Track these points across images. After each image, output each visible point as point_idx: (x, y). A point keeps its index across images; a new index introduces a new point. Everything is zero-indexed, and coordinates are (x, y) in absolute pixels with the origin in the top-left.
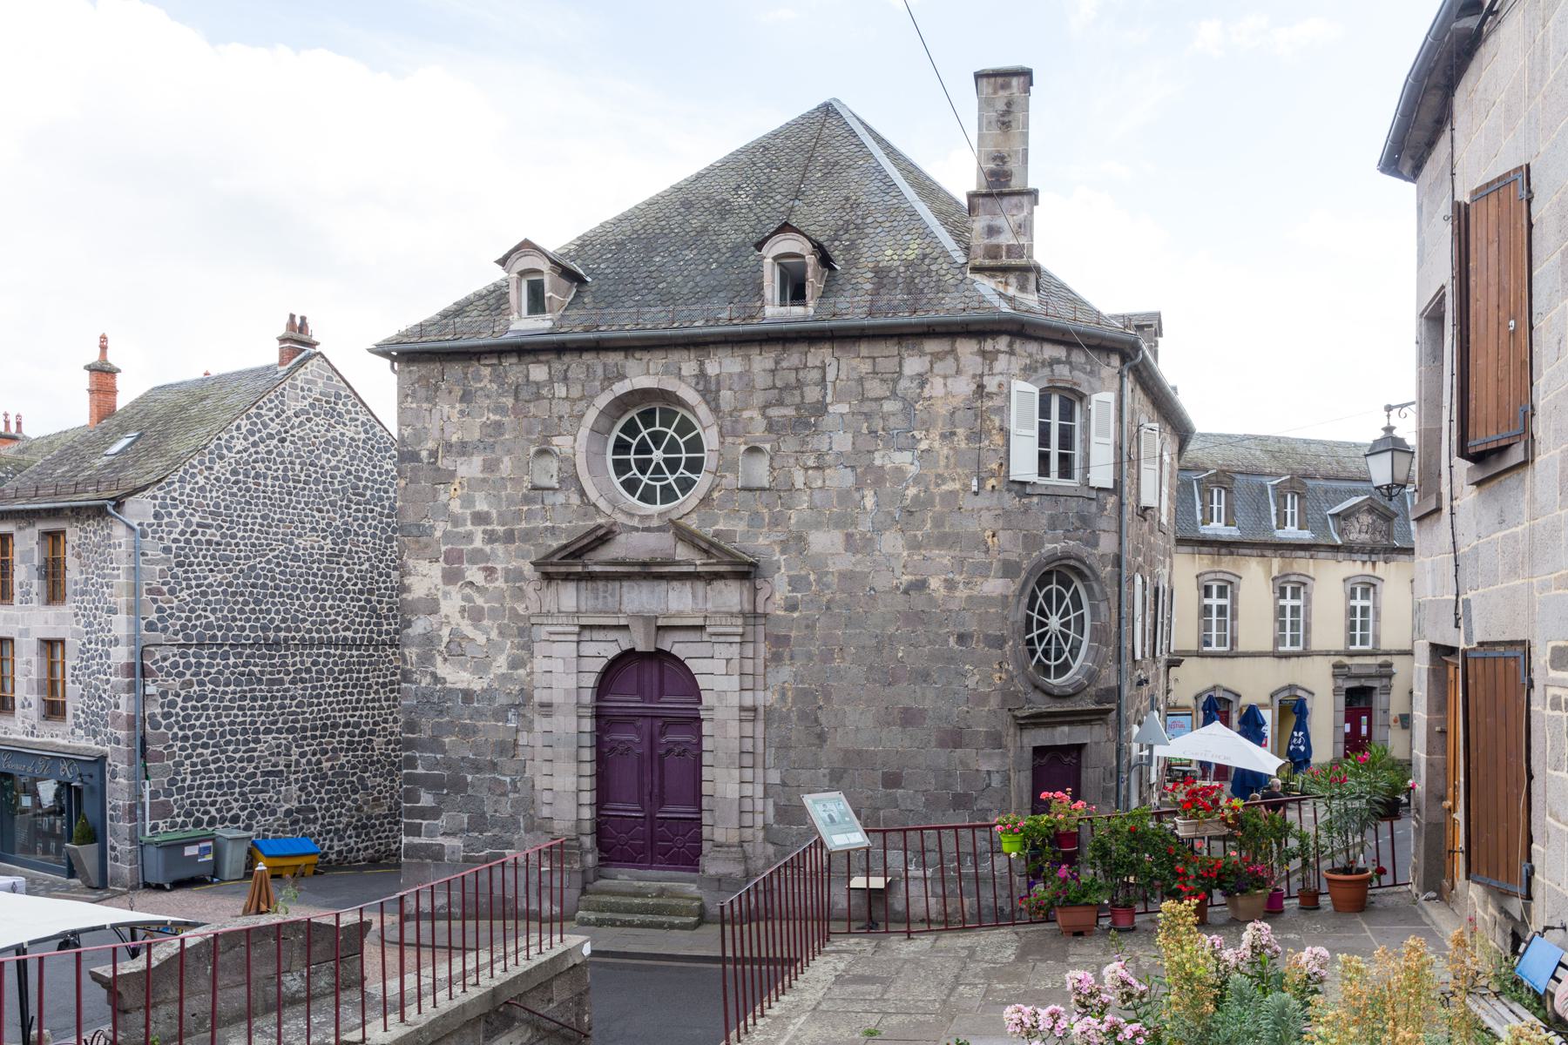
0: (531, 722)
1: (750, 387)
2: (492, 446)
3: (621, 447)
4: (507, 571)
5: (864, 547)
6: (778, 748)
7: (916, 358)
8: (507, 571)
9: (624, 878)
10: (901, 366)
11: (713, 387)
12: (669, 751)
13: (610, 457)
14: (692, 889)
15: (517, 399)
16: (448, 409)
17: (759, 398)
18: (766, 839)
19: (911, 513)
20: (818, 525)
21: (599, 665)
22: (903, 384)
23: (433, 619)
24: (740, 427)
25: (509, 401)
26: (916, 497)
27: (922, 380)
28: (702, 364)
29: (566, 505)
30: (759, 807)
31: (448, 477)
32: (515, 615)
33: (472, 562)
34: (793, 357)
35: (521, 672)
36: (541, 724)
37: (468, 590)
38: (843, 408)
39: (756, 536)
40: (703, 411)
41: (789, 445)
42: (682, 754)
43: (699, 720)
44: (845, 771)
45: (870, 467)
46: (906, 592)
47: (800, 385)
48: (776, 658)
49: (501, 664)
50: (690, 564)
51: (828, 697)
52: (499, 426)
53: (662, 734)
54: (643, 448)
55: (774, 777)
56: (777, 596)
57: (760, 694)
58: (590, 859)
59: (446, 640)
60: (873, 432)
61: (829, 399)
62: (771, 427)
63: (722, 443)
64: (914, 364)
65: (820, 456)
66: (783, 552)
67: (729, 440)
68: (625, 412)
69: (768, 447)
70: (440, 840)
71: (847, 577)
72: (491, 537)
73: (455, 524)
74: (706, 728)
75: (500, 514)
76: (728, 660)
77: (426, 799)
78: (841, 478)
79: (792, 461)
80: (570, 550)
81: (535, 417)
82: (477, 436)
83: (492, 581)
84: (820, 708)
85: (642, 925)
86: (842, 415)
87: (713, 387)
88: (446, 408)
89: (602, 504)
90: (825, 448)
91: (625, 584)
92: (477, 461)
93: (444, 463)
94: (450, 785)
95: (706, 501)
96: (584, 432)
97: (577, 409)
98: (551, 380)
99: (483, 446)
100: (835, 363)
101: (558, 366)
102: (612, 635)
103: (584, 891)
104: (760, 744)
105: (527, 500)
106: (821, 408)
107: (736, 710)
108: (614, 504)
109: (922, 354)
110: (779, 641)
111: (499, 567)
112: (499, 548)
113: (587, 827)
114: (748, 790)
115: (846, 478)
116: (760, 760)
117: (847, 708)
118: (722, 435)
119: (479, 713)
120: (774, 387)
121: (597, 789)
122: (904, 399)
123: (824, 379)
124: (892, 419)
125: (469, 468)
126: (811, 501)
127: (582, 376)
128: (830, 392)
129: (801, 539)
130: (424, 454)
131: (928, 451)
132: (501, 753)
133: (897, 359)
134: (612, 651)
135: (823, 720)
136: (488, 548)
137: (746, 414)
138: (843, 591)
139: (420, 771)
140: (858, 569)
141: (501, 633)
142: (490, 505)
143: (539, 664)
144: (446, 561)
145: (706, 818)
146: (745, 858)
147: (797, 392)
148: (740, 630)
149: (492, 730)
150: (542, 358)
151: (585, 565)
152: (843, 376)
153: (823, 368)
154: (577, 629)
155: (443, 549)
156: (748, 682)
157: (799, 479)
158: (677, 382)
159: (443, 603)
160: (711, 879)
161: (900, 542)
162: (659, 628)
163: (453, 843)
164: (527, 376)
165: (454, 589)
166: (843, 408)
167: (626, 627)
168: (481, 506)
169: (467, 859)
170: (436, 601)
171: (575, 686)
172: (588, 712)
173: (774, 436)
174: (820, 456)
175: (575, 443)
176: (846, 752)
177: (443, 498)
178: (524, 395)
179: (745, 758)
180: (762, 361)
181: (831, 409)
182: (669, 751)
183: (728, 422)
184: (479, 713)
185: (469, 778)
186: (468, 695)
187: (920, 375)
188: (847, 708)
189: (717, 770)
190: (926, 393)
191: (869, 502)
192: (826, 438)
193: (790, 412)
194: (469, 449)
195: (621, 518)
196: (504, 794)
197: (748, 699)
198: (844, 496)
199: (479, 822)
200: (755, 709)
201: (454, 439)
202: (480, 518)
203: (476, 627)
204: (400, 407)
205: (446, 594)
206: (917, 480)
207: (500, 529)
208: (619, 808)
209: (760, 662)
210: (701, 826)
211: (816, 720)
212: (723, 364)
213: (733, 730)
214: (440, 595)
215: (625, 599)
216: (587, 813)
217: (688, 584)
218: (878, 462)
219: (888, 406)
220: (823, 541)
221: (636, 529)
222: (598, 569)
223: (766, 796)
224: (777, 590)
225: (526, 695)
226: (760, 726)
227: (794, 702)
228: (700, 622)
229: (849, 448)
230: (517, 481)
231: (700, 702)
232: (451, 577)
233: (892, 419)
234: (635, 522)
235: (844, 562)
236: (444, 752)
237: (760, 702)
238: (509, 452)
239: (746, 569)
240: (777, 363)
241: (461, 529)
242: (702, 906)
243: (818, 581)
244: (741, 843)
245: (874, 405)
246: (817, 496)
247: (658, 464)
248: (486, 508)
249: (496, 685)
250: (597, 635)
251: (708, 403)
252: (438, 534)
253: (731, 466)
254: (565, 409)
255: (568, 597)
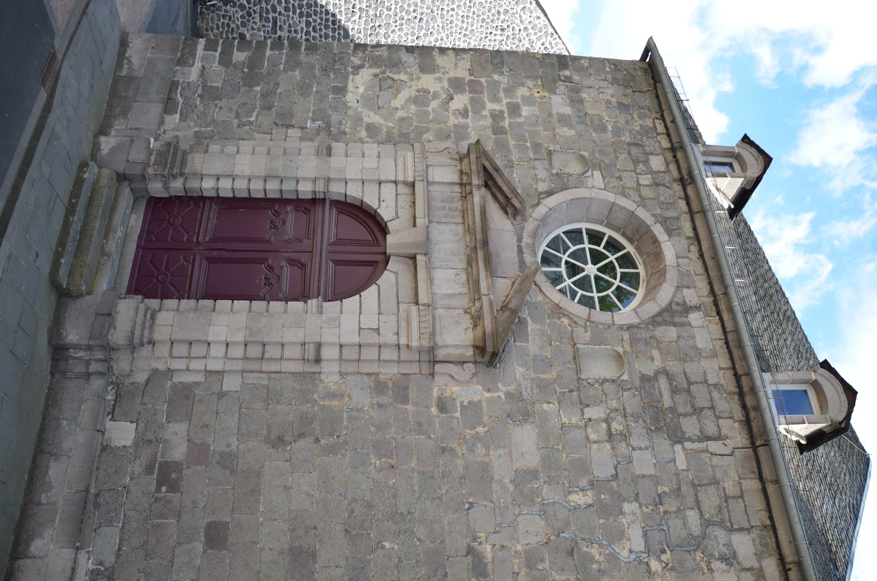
0: (311, 140)
1: (683, 359)
2: (583, 123)
3: (595, 237)
4: (466, 127)
5: (522, 493)
6: (267, 387)
7: (752, 550)
8: (466, 127)
9: (130, 223)
10: (741, 530)
11: (677, 320)
12: (271, 268)
13: (584, 226)
14: (103, 285)
15: (630, 144)
16: (610, 92)
17: (674, 366)
18: (155, 372)
19: (571, 553)
20: (544, 435)
21: (370, 200)
22: (721, 534)
23: (415, 69)
24: (641, 346)
25: (626, 138)
26: (592, 560)
27: (730, 559)
28: (697, 308)
29: (536, 179)
30: (196, 365)
31: (550, 86)
32: (420, 132)
33: (472, 100)
34: (729, 405)
35: (364, 134)
36: (308, 147)
37: (444, 96)
38: (682, 463)
39: (524, 364)
40: (652, 309)
41: (632, 402)
42: (268, 282)
43: (304, 296)
44: (233, 472)
45: (620, 498)
46: (470, 551)
47: (697, 411)
48: (380, 387)
49: (372, 117)
50: (491, 287)
51: (331, 450)
52: (604, 129)
53: (292, 262)
54: (597, 257)
55: (231, 384)
56: (455, 389)
57: (335, 367)
58: (156, 188)
59: (396, 77)
60: (660, 499)
61: (688, 445)
62: (645, 379)
63: (621, 327)
64: (745, 546)
65: (625, 436)
66: (508, 395)
67: (626, 336)
68: (631, 240)
69: (625, 377)
70: (198, 64)
71: (484, 471)
72: (496, 117)
73: (505, 90)
74: (295, 306)
75: (520, 125)
76: (377, 331)
77: (239, 56)
78: (602, 460)
79: (614, 404)
80: (494, 174)
81: (617, 158)
82: (590, 112)
83: (454, 114)
84: (317, 440)
85: (66, 226)
86: (674, 460)
87: (677, 320)
88: (611, 91)
89: (541, 210)
90: (635, 442)
91: (461, 227)
92: (568, 110)
93: (561, 87)
94: (252, 73)
95: (558, 311)
96: (611, 197)
97: (631, 192)
98: (652, 173)
99: (583, 117)
100: (728, 451)
101: (667, 178)
102: (405, 214)
103: (122, 178)
104: (274, 367)
105: (537, 147)
106: (678, 438)
107: (317, 339)
108: (543, 221)
109: (759, 556)
110: (401, 392)
111: (469, 121)
112: (488, 122)
113: (194, 184)
114: (217, 351)
115: (603, 470)
116: (254, 366)
117: (315, 475)
118: (630, 327)
119: (321, 97)
120: (690, 383)
121: (234, 199)
122: (704, 536)
123: (709, 438)
124: (679, 523)
125: (559, 103)
126: (572, 427)
127: (662, 198)
128: (696, 446)
129: (526, 416)
130: (567, 73)
131: (649, 571)
132: (281, 115)
133: (746, 525)
134: (386, 213)
135: (302, 443)
136: (485, 113)
137: (656, 353)
138: (466, 468)
139: (268, 52)
140: (495, 487)
141: (402, 119)
142: (526, 117)
143: (371, 149)
144: (470, 81)
145: (187, 304)
146: (132, 347)
147: (689, 409)
148: (415, 344)
149: (304, 109)
150: (673, 167)
151: (479, 187)
152: (716, 460)
153: (719, 438)
154: (410, 179)
155: (483, 80)
156: (350, 354)
157: (595, 412)
158: (675, 284)
159: (431, 76)
160: (114, 306)
161: (533, 540)
162: (413, 258)
163: (193, 74)
164: (652, 154)
165: (446, 84)
166: (682, 463)
167: (415, 225)
168: (525, 111)
169: (174, 85)
170: (433, 71)
171: (348, 177)
172: (320, 187)
173: (637, 383)
174: (625, 436)
175: (596, 188)
176: (259, 474)
177: (530, 83)
178: (635, 150)
179: (258, 348)
180: (715, 369)
181: (678, 448)
182: (271, 268)
183: (643, 334)
184: (321, 97)
185: (258, 89)
186: (341, 91)
187: (735, 556)
188: (315, 475)
189: (244, 316)
190: (717, 565)
191: (578, 499)
192: (644, 443)
193: (667, 402)
194: (577, 105)
195: (530, 226)
196: (237, 115)
197: (329, 353)
198: (582, 467)
199: (211, 94)
200: (318, 360)
201: (584, 95)
202: (514, 109)
203: (409, 100)
204: (605, 59)
205: (440, 80)
206: (613, 558)
207: (506, 123)
208: (211, 218)
209: (374, 368)
210: (180, 298)
211: (301, 435)
212: (703, 331)
213: (292, 335)
214: (437, 75)
215: (444, 227)
216: (208, 186)
217: (464, 290)
218: (627, 507)
219: (692, 516)
220: (526, 442)
221: (520, 240)
222: (477, 199)
223: (208, 373)
224: (465, 388)
225: (341, 136)
226: (297, 367)
227: (323, 408)
228: (423, 298)
229: (638, 472)
230: (554, 139)
231: (326, 299)
232: (457, 85)
233: (679, 523)
234: (526, 239)
235: (502, 469)
236: (285, 71)
237: (325, 367)
238: (579, 135)
239: (489, 349)
240: (715, 386)
241: (502, 94)
242: (80, 295)
243: (477, 437)
244: (152, 342)
245: (690, 500)
246: (578, 434)
247: (583, 270)
248: (524, 114)
249: (350, 113)
250: (404, 201)
251: (660, 314)
252: (496, 77)
253: (598, 339)
254: (629, 181)
255: (445, 174)
